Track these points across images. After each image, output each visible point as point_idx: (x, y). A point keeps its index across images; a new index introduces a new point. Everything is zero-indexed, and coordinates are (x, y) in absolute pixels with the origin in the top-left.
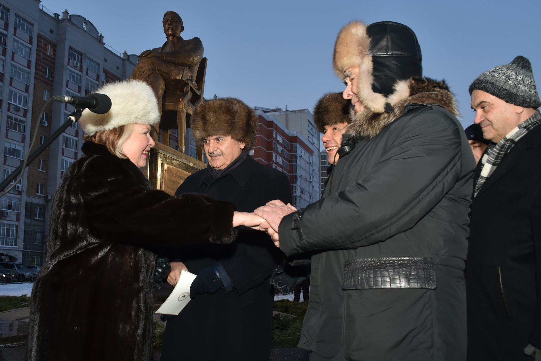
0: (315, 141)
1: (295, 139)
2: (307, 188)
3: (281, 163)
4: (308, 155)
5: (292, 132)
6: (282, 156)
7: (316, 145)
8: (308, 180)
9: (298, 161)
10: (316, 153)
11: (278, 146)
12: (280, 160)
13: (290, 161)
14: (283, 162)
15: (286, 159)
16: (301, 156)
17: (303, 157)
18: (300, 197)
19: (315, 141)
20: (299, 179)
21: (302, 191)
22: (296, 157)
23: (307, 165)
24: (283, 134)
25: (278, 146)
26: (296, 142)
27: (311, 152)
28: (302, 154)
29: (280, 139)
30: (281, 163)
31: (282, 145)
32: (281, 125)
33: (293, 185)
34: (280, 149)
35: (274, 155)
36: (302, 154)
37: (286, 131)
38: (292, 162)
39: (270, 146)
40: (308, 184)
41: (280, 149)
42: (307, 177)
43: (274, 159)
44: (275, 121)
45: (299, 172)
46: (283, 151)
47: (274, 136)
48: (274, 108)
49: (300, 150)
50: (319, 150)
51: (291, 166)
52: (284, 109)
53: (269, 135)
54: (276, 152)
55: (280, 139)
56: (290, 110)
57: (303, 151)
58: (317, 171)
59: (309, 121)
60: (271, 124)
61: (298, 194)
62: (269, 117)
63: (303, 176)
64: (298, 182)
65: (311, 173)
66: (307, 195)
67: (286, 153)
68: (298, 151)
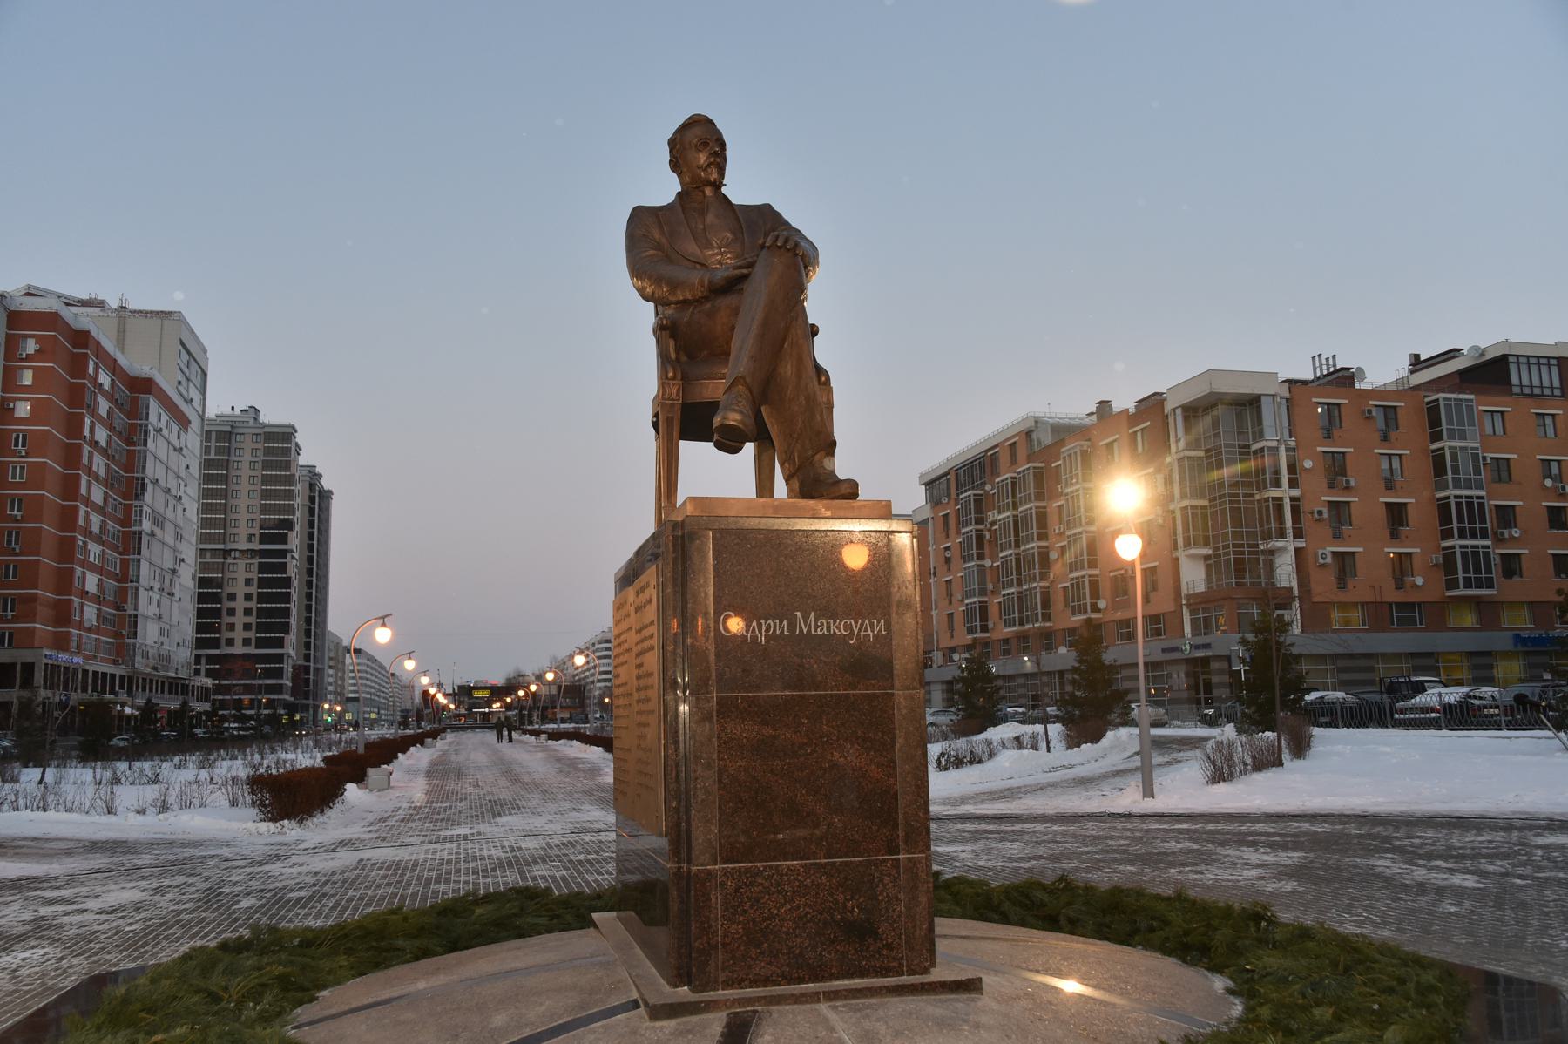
0: (194, 394)
1: (144, 386)
2: (169, 514)
3: (103, 444)
4: (176, 428)
5: (136, 362)
6: (111, 428)
7: (196, 403)
8: (174, 492)
9: (150, 441)
10: (195, 423)
11: (100, 399)
12: (101, 435)
13: (129, 442)
14: (109, 442)
15: (119, 435)
16: (159, 431)
17: (165, 432)
18: (152, 534)
19: (194, 394)
20: (150, 487)
21: (158, 520)
22: (146, 432)
23: (174, 455)
24: (114, 367)
25: (100, 399)
26: (149, 392)
27: (184, 422)
28: (163, 424)
29: (105, 380)
30: (103, 444)
31: (110, 397)
32: (108, 345)
33: (136, 503)
34: (104, 406)
35: (87, 421)
36: (163, 424)
37: (123, 361)
38: (134, 444)
39: (77, 396)
40: (172, 502)
41: (104, 406)
42: (172, 484)
43: (87, 433)
44: (94, 333)
45: (152, 470)
46: (110, 412)
47: (91, 371)
48: (85, 297)
49: (156, 415)
50: (202, 417)
51: (131, 454)
52: (114, 304)
53: (77, 366)
54: (94, 411)
55: (105, 380)
56: (131, 307)
57: (165, 418)
58: (195, 470)
59: (182, 344)
60: (82, 338)
61: (146, 525)
62: (81, 319)
63: (162, 483)
64: (148, 497)
65: (183, 473)
66: (169, 527)
67: (120, 419)
68: (153, 418)
